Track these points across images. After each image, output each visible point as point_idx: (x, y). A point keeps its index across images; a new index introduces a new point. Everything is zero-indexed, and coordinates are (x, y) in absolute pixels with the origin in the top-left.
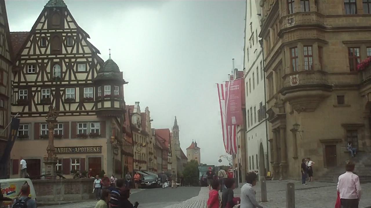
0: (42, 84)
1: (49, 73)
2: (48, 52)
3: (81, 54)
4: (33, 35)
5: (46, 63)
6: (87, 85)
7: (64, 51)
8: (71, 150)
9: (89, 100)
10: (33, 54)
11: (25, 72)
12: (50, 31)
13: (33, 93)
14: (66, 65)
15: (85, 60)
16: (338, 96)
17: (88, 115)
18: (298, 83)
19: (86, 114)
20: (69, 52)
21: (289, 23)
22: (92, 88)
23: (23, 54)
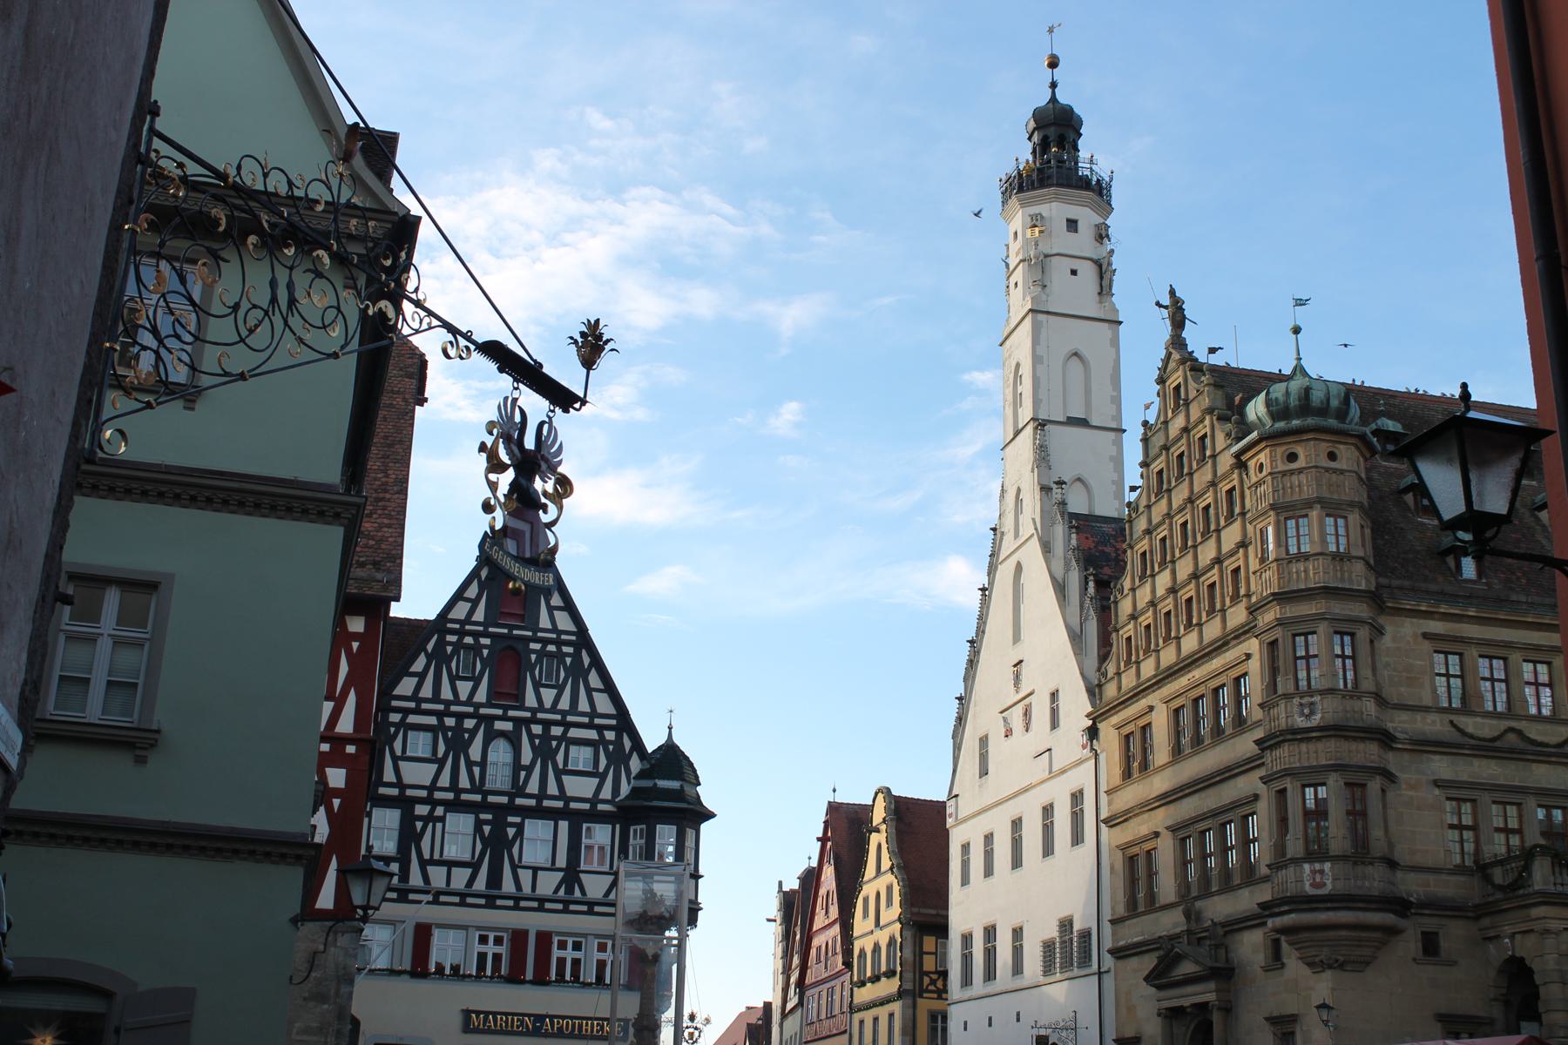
0: (450, 796)
1: (476, 764)
2: (481, 696)
3: (583, 714)
5: (467, 730)
7: (530, 700)
11: (399, 752)
13: (419, 825)
15: (592, 734)
16: (1423, 933)
17: (590, 912)
18: (1329, 883)
19: (585, 908)
20: (548, 704)
21: (1302, 714)
23: (397, 692)
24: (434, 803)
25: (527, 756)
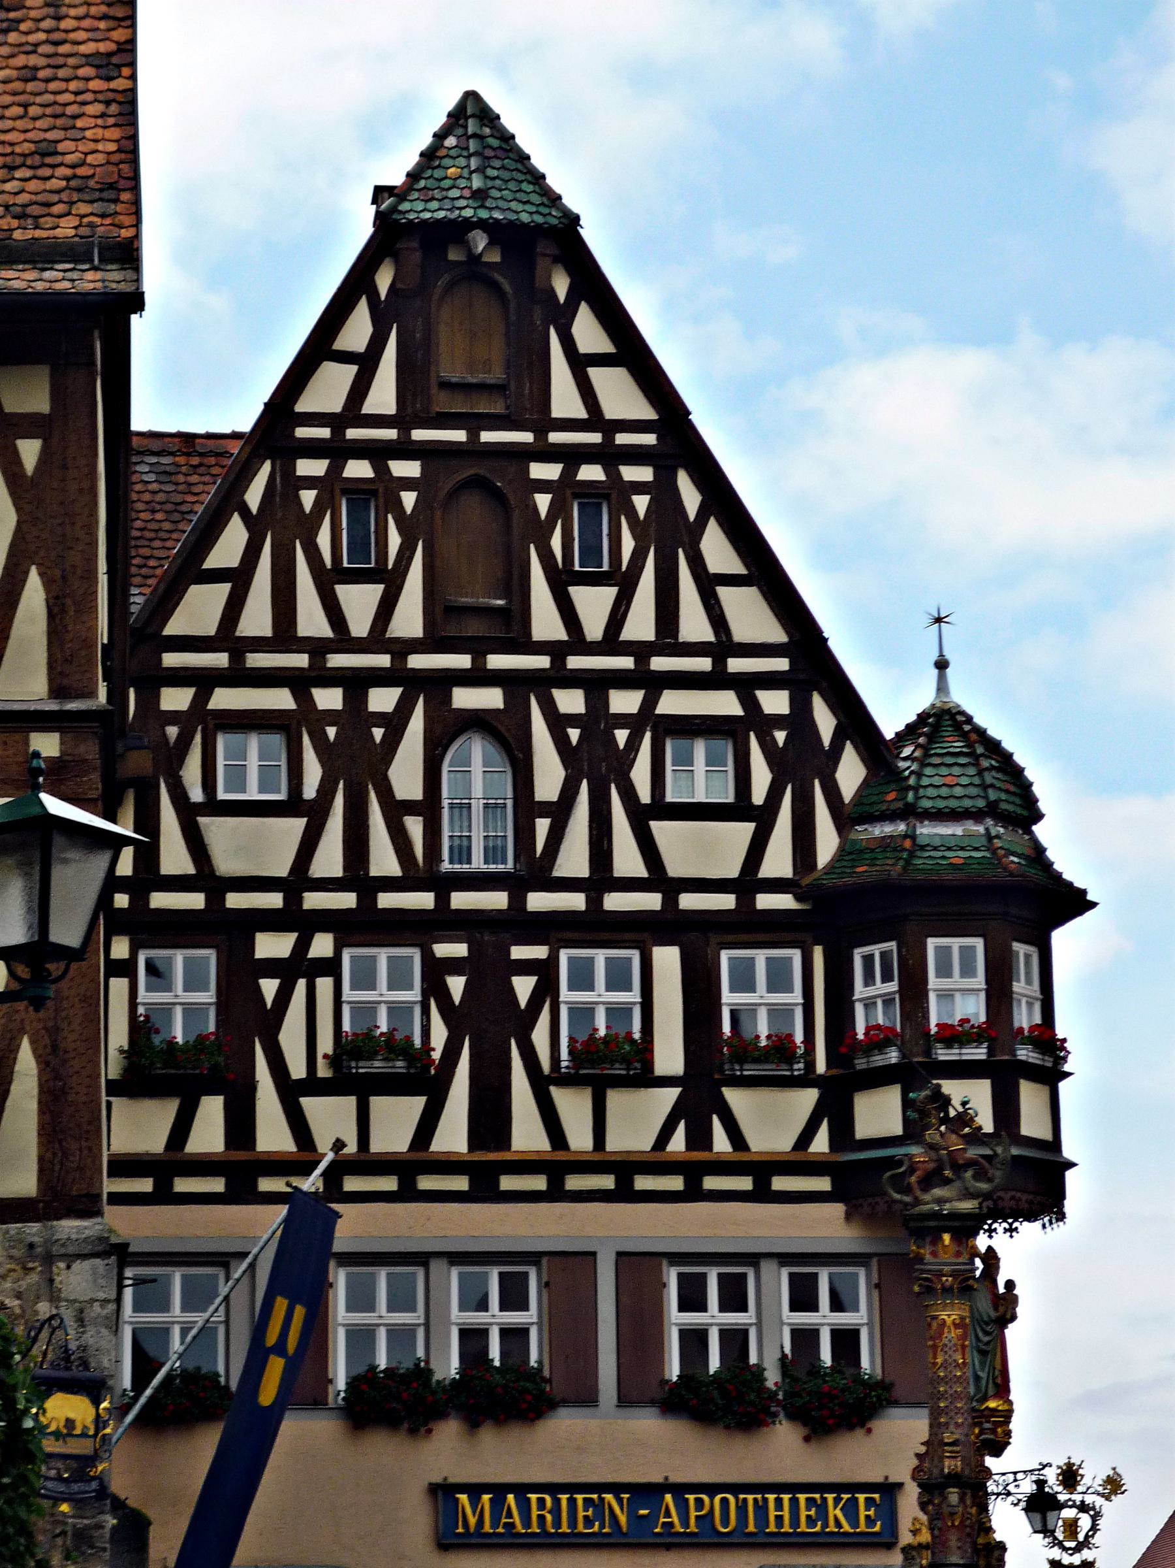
0: (347, 900)
1: (410, 807)
4: (267, 467)
5: (381, 719)
6: (749, 927)
7: (546, 622)
8: (623, 1519)
9: (777, 1064)
10: (268, 632)
11: (196, 795)
12: (418, 435)
13: (269, 987)
14: (561, 742)
15: (726, 704)
17: (762, 1194)
19: (744, 1183)
20: (594, 629)
22: (796, 955)
24: (305, 924)
25: (549, 776)
